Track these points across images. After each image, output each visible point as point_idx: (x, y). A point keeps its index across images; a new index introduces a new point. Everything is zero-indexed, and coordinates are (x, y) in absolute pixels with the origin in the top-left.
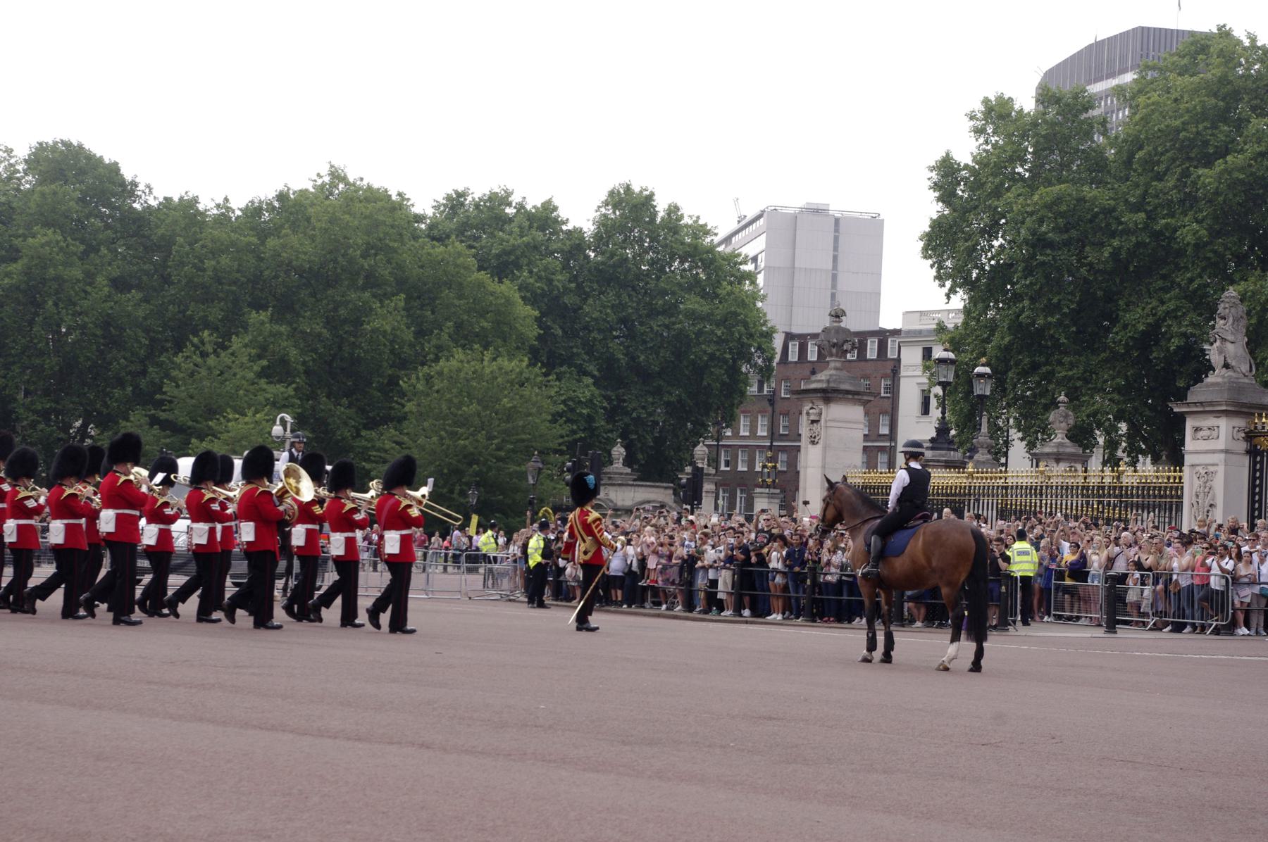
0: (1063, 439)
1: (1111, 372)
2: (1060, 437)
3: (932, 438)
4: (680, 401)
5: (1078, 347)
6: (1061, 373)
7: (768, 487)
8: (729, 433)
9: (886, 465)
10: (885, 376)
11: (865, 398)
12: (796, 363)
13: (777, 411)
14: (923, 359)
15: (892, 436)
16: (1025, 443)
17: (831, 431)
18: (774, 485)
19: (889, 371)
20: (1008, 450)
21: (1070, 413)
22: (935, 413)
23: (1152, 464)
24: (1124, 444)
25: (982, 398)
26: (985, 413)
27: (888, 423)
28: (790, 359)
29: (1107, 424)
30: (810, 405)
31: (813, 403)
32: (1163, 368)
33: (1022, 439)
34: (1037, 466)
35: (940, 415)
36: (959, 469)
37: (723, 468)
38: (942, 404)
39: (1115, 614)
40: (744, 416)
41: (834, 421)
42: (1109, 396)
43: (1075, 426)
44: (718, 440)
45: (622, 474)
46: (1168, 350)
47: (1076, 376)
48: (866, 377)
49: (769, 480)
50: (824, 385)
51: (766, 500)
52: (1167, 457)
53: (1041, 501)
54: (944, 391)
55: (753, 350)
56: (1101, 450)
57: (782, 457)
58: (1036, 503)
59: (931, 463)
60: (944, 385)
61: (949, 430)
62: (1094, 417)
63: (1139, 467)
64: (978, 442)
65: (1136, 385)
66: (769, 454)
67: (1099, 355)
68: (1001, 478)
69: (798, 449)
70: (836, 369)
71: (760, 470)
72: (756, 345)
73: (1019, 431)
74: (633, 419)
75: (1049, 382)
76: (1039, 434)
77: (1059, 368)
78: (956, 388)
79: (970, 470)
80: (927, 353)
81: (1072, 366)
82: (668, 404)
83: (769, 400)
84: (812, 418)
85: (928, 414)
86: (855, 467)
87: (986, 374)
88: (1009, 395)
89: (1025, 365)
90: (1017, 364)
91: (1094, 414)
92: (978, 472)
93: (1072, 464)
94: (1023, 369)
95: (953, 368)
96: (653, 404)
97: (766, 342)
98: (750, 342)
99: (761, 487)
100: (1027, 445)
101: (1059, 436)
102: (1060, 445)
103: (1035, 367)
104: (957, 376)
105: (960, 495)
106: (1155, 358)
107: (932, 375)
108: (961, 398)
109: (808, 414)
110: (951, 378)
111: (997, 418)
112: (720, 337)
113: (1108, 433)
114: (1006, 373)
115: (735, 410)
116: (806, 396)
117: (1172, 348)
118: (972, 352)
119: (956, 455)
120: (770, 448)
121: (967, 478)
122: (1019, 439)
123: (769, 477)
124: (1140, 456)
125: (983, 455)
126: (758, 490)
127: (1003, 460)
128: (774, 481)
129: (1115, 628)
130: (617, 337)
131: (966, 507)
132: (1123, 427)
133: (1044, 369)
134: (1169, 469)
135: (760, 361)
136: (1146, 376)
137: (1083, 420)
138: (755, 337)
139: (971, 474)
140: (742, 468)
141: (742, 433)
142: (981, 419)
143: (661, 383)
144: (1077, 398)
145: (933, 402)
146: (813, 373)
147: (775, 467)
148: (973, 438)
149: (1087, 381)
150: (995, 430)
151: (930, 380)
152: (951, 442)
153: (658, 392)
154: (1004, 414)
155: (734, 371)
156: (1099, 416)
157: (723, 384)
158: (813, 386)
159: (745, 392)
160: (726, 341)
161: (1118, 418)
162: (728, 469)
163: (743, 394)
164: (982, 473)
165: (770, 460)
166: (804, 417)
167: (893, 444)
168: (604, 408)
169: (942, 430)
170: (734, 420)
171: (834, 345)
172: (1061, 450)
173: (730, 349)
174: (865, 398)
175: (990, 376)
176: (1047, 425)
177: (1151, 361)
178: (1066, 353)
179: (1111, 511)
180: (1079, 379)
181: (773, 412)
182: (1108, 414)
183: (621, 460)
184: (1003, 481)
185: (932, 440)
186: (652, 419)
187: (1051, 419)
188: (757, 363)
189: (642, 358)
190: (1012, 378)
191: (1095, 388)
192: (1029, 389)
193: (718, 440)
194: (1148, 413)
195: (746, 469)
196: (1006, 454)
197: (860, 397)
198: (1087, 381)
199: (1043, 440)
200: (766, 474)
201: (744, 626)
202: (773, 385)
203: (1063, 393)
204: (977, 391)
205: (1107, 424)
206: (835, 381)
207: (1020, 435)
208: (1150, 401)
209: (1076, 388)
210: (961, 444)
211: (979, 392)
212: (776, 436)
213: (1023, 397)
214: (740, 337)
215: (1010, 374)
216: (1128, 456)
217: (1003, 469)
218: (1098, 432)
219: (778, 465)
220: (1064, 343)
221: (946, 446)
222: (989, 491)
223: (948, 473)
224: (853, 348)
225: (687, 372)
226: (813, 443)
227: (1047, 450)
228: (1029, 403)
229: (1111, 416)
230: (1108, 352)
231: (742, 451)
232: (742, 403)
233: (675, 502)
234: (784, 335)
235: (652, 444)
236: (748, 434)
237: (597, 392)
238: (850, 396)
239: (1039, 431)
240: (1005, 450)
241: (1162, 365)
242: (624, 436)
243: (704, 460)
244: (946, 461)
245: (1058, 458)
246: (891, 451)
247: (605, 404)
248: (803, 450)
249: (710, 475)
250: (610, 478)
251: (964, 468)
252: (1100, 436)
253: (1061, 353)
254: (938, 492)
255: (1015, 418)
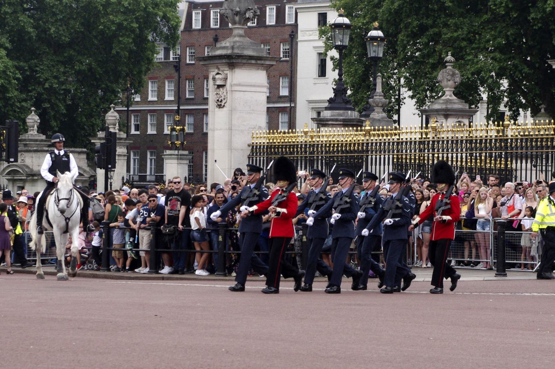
0: (451, 96)
1: (493, 33)
2: (449, 95)
3: (331, 99)
4: (90, 69)
5: (462, 10)
6: (447, 35)
7: (177, 149)
8: (138, 98)
9: (286, 125)
10: (283, 41)
11: (268, 63)
12: (199, 30)
13: (183, 76)
14: (319, 25)
15: (292, 97)
16: (415, 100)
17: (237, 95)
18: (182, 147)
19: (287, 36)
20: (399, 107)
21: (457, 72)
22: (332, 74)
23: (532, 116)
24: (506, 99)
25: (376, 59)
26: (379, 74)
27: (287, 84)
28: (194, 27)
29: (490, 81)
30: (216, 71)
31: (219, 69)
32: (540, 28)
33: (412, 97)
34: (427, 123)
35: (337, 77)
36: (357, 126)
37: (133, 132)
38: (338, 65)
39: (504, 259)
40: (152, 82)
41: (239, 85)
42: (492, 55)
43: (462, 84)
44: (128, 106)
45: (36, 140)
46: (544, 11)
47: (461, 37)
48: (265, 42)
49: (178, 143)
50: (229, 52)
51: (176, 161)
52: (545, 110)
53: (433, 155)
54: (340, 55)
55: (159, 20)
56: (485, 106)
57: (189, 120)
58: (428, 157)
59: (330, 123)
60: (339, 48)
61: (345, 91)
62: (478, 75)
63: (520, 120)
64: (374, 102)
65: (516, 44)
66: (177, 118)
67: (481, 17)
68: (395, 135)
69: (205, 112)
70: (240, 36)
71: (169, 132)
72: (161, 14)
73: (409, 90)
74: (45, 89)
75: (437, 43)
76: (428, 92)
77: (445, 30)
78: (351, 51)
79: (368, 128)
80: (323, 18)
81: (457, 27)
82: (78, 73)
83: (175, 67)
84: (219, 83)
85: (325, 76)
86: (260, 128)
87: (379, 37)
88: (399, 56)
89: (414, 27)
90: (406, 27)
91: (478, 72)
92: (374, 130)
93: (460, 120)
94: (412, 31)
95: (348, 32)
96: (64, 73)
97: (170, 11)
98: (156, 11)
99: (171, 149)
100: (417, 102)
101: (447, 93)
102: (448, 101)
103: (423, 29)
104: (351, 39)
105: (358, 151)
106: (533, 19)
107: (328, 39)
108: (356, 60)
109: (214, 79)
110: (346, 42)
111: (389, 78)
112: (127, 8)
113: (490, 89)
114: (396, 35)
115: (143, 77)
116: (212, 62)
117: (548, 9)
118: (364, 17)
119: (354, 114)
120: (178, 112)
121: (365, 135)
122: (409, 97)
123: (177, 140)
124: (521, 110)
125: (378, 113)
126: (168, 152)
127: (395, 117)
128: (182, 144)
129: (505, 271)
130: (29, 10)
131: (364, 163)
132: (505, 83)
133: (431, 32)
134: (550, 121)
135: (165, 29)
136: (525, 35)
137: (468, 78)
138: (161, 7)
139: (368, 132)
140: (151, 131)
141: (150, 99)
142: (375, 79)
143: (72, 52)
144: (463, 58)
145: (330, 65)
146: (216, 40)
147: (183, 130)
148: (369, 98)
149: (471, 42)
150: (388, 88)
151: (326, 44)
152: (348, 102)
153: (69, 62)
154: (395, 74)
155: (141, 40)
156: (483, 74)
157: (131, 52)
158: (218, 52)
159: (152, 59)
160: (133, 11)
161: (500, 75)
162: (138, 133)
163: (150, 61)
164: (379, 130)
165: (177, 123)
166: (211, 82)
167: (293, 105)
168: (18, 79)
169: (339, 91)
170: (143, 87)
171: (237, 13)
172: (449, 106)
173: (137, 18)
174: (268, 63)
175: (382, 39)
176: (435, 84)
177: (529, 21)
178: (451, 16)
179: (493, 162)
180: (463, 39)
181: (179, 77)
182: (491, 71)
183: (36, 127)
184: (397, 137)
185: (331, 101)
186: (63, 87)
187: (440, 78)
188: (161, 32)
189: (53, 30)
190: (402, 40)
191: (478, 48)
192: (418, 50)
193: (128, 106)
194: (526, 70)
195: (155, 132)
196: (398, 112)
197: (263, 62)
198: (471, 42)
199: (432, 97)
200: (175, 137)
201: (161, 283)
202: (179, 52)
203: (450, 53)
204: (371, 53)
205: (490, 81)
206: (238, 48)
207: (410, 93)
208: (529, 59)
209: (461, 49)
210: (356, 104)
211: (373, 55)
212: (182, 100)
213: (412, 57)
214: (146, 7)
215: (400, 37)
216: (510, 110)
217: (396, 125)
218: (482, 89)
219: (186, 128)
220: (449, 6)
221: (343, 105)
222: (382, 148)
223: (346, 131)
224: (255, 15)
225: (96, 42)
226: (220, 106)
227: (436, 106)
228: (418, 63)
229: (493, 74)
230: (489, 13)
231: (151, 116)
232: (149, 69)
233: (89, 166)
234: (188, 4)
235: (65, 111)
236: (155, 99)
237: (10, 63)
238: (253, 62)
239: (428, 89)
240: (397, 107)
241: (540, 25)
242: (37, 105)
243: (115, 125)
244: (344, 120)
245: (447, 114)
246: (291, 112)
247: (19, 76)
248: (210, 113)
249: (121, 139)
250: (25, 145)
251: (361, 126)
252: (484, 92)
253: (447, 15)
254: (338, 150)
255: (406, 77)
